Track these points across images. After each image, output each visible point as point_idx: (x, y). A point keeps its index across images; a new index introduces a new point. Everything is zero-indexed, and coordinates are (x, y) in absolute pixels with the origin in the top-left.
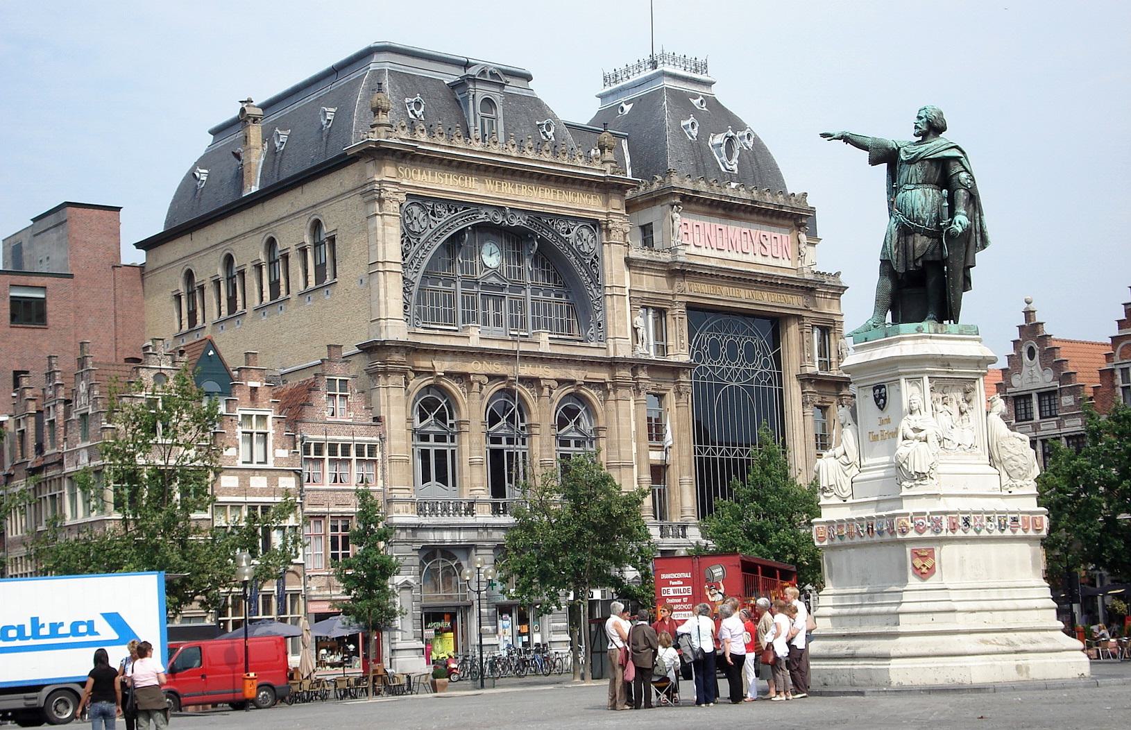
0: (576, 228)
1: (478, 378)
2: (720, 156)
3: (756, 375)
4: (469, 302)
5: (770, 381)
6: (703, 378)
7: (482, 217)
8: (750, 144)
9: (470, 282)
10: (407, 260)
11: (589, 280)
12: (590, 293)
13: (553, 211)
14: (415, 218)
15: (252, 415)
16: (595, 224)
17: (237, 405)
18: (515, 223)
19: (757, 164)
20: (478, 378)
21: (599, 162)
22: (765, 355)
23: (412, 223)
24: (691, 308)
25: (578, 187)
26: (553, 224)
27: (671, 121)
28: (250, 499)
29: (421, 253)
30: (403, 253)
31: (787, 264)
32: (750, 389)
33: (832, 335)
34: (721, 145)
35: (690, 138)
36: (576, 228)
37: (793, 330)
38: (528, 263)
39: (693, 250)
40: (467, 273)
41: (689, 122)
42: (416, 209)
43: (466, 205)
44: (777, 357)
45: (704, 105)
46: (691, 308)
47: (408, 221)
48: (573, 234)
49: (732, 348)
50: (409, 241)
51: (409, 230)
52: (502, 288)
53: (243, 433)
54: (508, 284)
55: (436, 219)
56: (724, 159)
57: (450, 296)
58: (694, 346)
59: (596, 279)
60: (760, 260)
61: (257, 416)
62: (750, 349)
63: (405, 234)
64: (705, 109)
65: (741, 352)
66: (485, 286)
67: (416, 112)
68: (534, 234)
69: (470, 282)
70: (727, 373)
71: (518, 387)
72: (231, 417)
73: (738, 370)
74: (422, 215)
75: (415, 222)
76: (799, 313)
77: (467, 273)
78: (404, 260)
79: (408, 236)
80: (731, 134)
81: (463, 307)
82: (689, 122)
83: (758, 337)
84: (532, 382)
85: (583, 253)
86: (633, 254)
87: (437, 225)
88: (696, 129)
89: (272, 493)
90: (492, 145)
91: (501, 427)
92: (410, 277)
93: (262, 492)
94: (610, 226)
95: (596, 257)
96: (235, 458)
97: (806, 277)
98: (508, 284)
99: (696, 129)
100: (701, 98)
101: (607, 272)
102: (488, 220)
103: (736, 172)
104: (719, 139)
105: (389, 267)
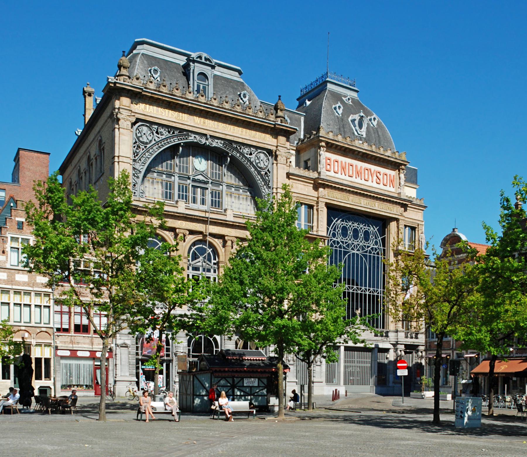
0: (257, 152)
1: (182, 231)
2: (355, 126)
3: (369, 248)
4: (183, 189)
5: (378, 254)
6: (336, 247)
7: (192, 138)
8: (375, 123)
9: (184, 177)
10: (137, 158)
11: (263, 183)
12: (263, 190)
13: (240, 140)
14: (144, 134)
15: (18, 238)
16: (270, 152)
17: (7, 231)
18: (214, 144)
19: (378, 134)
20: (182, 231)
21: (274, 116)
22: (376, 238)
23: (141, 136)
24: (328, 205)
25: (258, 129)
26: (241, 148)
27: (326, 104)
28: (14, 287)
29: (147, 154)
30: (134, 154)
31: (392, 189)
32: (365, 256)
33: (417, 232)
34: (355, 120)
35: (337, 114)
36: (257, 152)
37: (393, 224)
38: (225, 170)
39: (332, 173)
40: (183, 171)
41: (337, 106)
42: (145, 129)
43: (181, 130)
44: (383, 240)
45: (350, 101)
46: (328, 205)
47: (139, 135)
48: (253, 156)
49: (356, 232)
50: (139, 147)
51: (139, 140)
52: (206, 183)
53: (11, 248)
54: (210, 181)
55: (159, 136)
56: (357, 128)
57: (170, 184)
58: (332, 228)
59: (267, 184)
60: (375, 185)
61: (22, 239)
62: (367, 234)
63: (136, 142)
64: (351, 103)
65: (361, 235)
66: (194, 180)
67: (154, 75)
68: (228, 153)
69: (184, 177)
70: (351, 246)
71: (209, 239)
72: (2, 238)
73: (358, 245)
74: (149, 132)
75: (144, 136)
76: (397, 217)
77: (183, 171)
78: (135, 157)
79: (138, 143)
80: (362, 114)
81: (179, 191)
82: (337, 106)
83: (372, 228)
84: (221, 237)
85: (260, 168)
86: (291, 171)
87: (159, 140)
88: (341, 109)
89: (31, 285)
90: (200, 97)
91: (200, 262)
92: (137, 166)
93: (24, 284)
94: (278, 153)
95: (268, 170)
96: (6, 262)
97: (402, 197)
98: (210, 181)
99: (341, 109)
100: (348, 97)
101: (275, 180)
102: (195, 141)
103: (364, 136)
104: (357, 117)
105: (121, 159)
